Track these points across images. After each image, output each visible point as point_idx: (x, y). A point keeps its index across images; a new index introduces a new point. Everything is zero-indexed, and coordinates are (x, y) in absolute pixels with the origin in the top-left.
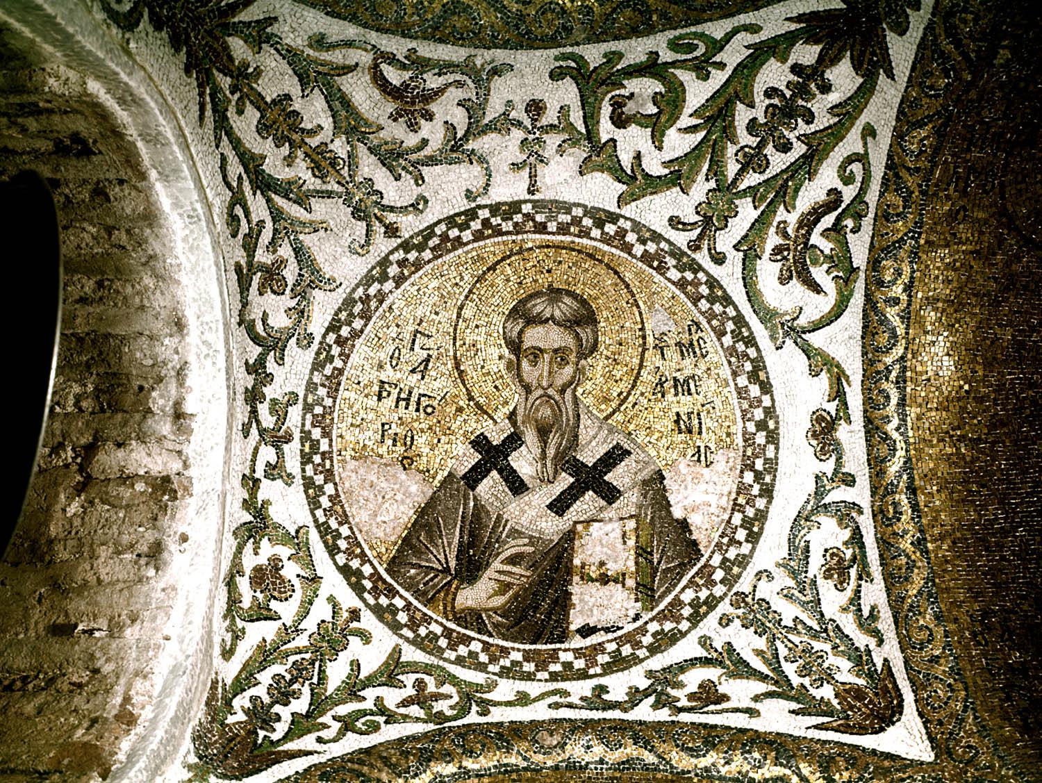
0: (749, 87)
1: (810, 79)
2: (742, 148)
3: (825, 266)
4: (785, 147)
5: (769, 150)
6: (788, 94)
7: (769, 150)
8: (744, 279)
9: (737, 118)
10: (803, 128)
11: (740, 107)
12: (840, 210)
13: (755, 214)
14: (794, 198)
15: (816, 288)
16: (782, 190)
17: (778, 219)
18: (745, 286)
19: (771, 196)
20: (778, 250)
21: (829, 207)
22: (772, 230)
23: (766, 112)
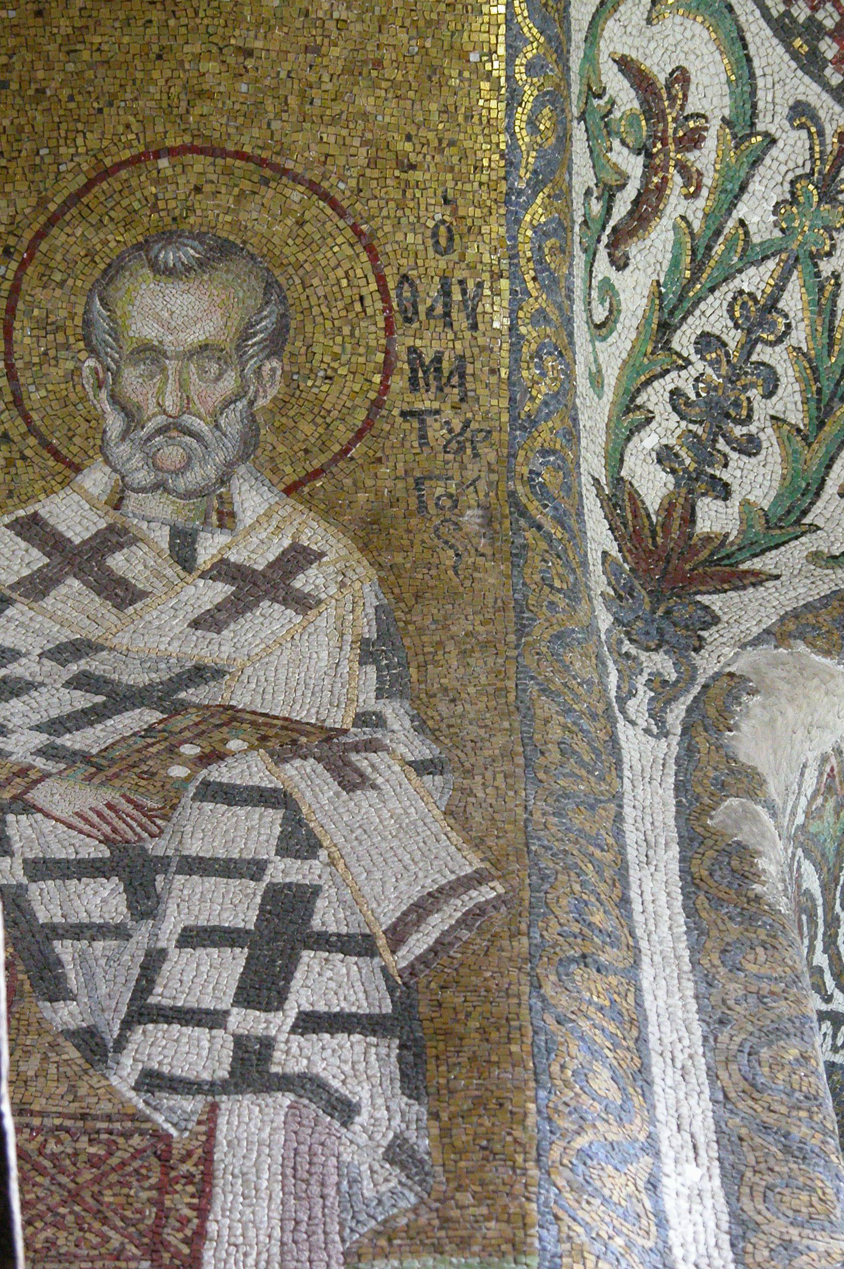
0: (790, 457)
1: (699, 478)
2: (779, 340)
3: (617, 114)
4: (706, 342)
5: (733, 338)
6: (721, 445)
7: (733, 338)
8: (752, 76)
9: (798, 397)
10: (683, 380)
11: (796, 417)
12: (608, 230)
13: (742, 210)
14: (677, 244)
15: (625, 65)
16: (701, 262)
17: (701, 203)
18: (749, 60)
19: (719, 249)
20: (693, 140)
21: (619, 237)
22: (707, 181)
23: (750, 410)
